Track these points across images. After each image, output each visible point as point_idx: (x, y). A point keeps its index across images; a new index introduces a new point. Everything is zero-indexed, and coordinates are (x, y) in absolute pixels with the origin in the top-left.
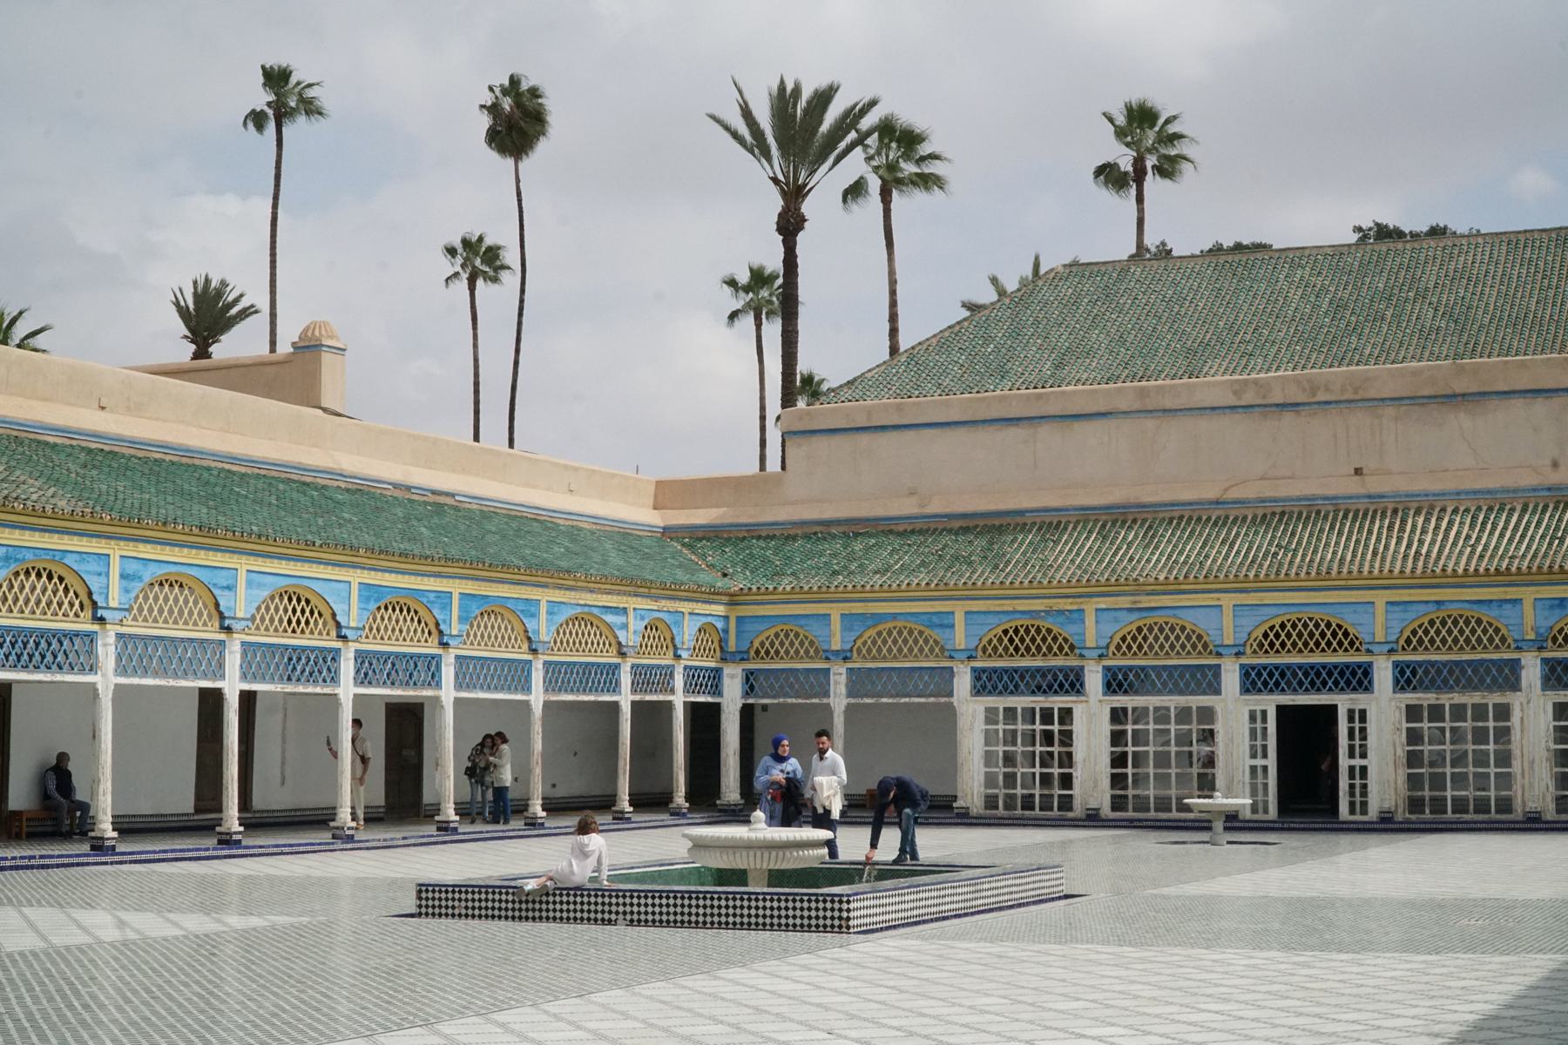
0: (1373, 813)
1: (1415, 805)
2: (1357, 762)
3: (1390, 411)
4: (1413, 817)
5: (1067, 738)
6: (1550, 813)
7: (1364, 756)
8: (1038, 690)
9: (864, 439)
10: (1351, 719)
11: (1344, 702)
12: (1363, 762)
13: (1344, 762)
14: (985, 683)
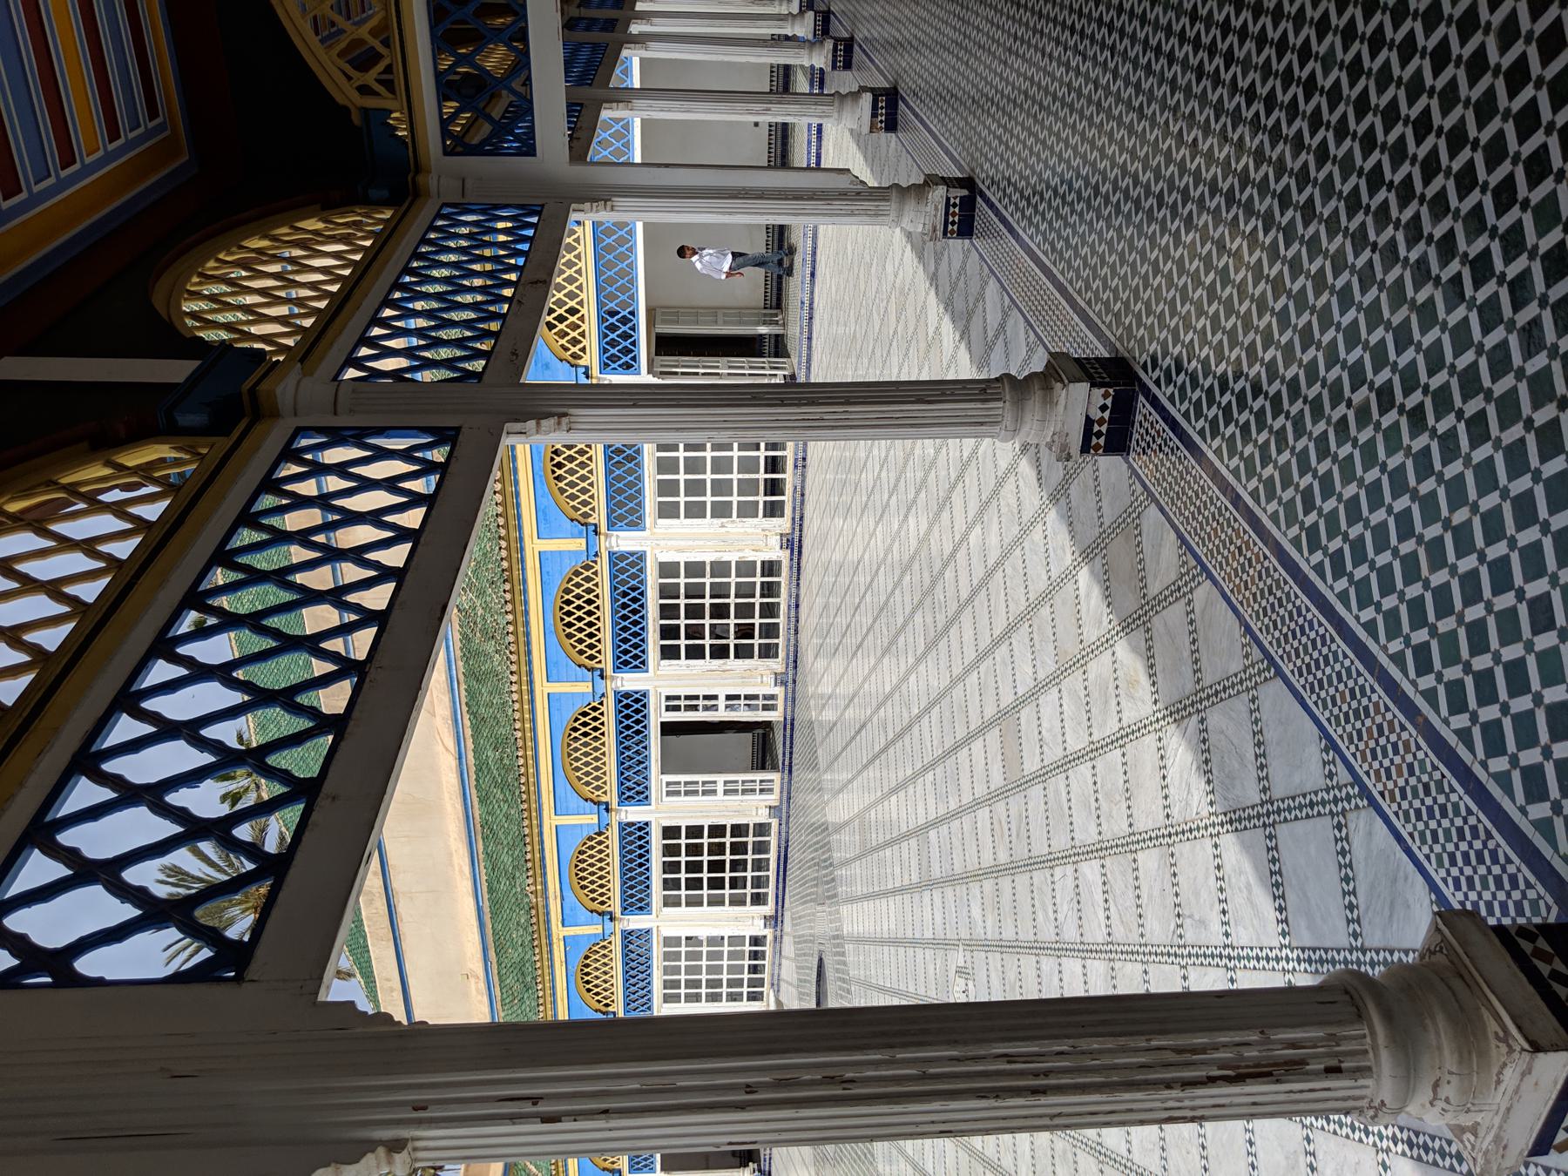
2: (722, 702)
4: (781, 654)
6: (783, 524)
10: (677, 708)
11: (657, 716)
12: (722, 698)
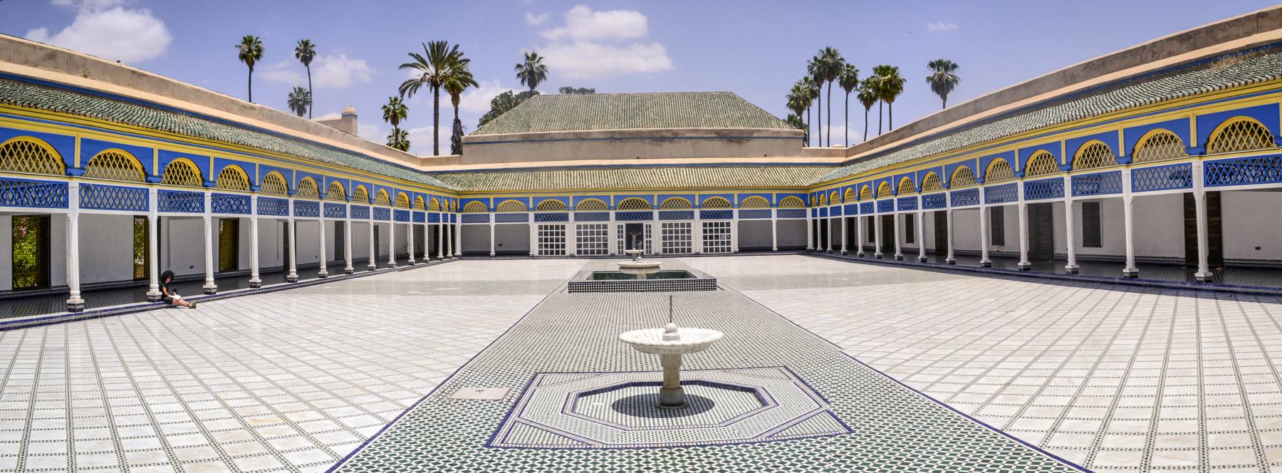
0: (653, 253)
1: (665, 251)
3: (647, 141)
5: (563, 234)
6: (702, 252)
7: (650, 237)
8: (545, 220)
9: (488, 145)
10: (647, 227)
11: (645, 223)
13: (645, 239)
14: (537, 218)
